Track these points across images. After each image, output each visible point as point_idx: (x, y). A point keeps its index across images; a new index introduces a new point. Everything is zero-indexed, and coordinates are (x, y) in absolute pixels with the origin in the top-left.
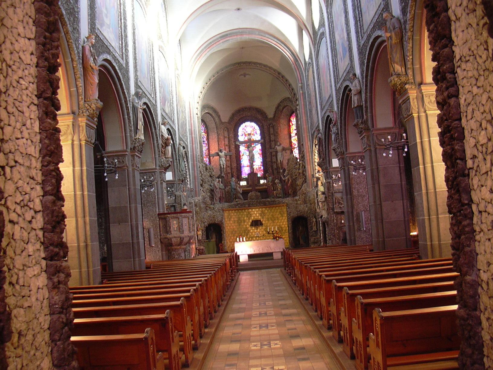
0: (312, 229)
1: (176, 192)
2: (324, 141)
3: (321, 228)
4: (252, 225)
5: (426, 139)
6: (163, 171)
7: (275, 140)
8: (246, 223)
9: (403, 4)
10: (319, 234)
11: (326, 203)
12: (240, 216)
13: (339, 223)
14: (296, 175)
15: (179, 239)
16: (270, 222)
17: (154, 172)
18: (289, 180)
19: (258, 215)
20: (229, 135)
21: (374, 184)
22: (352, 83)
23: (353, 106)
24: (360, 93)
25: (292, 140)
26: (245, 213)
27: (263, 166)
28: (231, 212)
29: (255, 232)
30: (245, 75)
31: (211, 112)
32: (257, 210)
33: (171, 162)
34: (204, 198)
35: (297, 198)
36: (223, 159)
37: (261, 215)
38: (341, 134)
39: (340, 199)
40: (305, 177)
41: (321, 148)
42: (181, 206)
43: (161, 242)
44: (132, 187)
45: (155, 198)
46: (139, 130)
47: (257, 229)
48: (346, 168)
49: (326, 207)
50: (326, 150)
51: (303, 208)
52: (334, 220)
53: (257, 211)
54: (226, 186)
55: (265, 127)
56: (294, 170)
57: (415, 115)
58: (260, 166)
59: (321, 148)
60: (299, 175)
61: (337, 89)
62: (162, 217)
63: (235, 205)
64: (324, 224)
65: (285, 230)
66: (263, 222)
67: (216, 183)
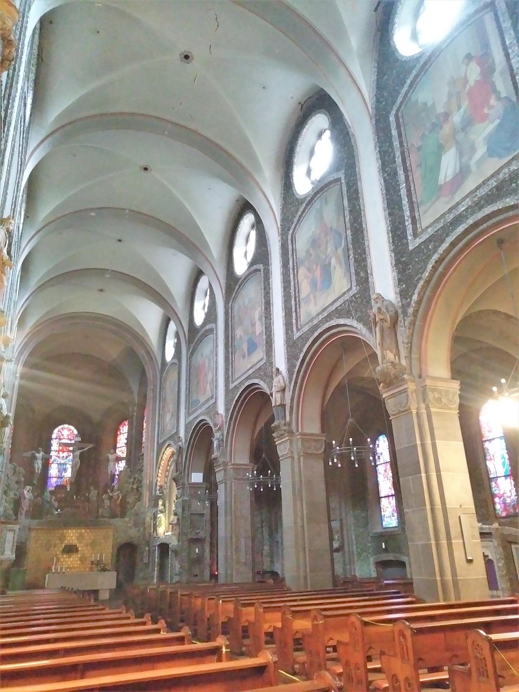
3: (156, 560)
5: (428, 441)
8: (56, 549)
9: (404, 286)
14: (128, 491)
16: (89, 548)
19: (74, 538)
21: (295, 500)
23: (273, 405)
24: (283, 390)
25: (117, 451)
26: (58, 535)
28: (39, 531)
32: (74, 531)
35: (127, 519)
38: (227, 440)
41: (180, 459)
48: (229, 483)
51: (133, 533)
53: (73, 533)
56: (126, 485)
57: (414, 412)
59: (180, 459)
66: (79, 549)
67: (25, 492)
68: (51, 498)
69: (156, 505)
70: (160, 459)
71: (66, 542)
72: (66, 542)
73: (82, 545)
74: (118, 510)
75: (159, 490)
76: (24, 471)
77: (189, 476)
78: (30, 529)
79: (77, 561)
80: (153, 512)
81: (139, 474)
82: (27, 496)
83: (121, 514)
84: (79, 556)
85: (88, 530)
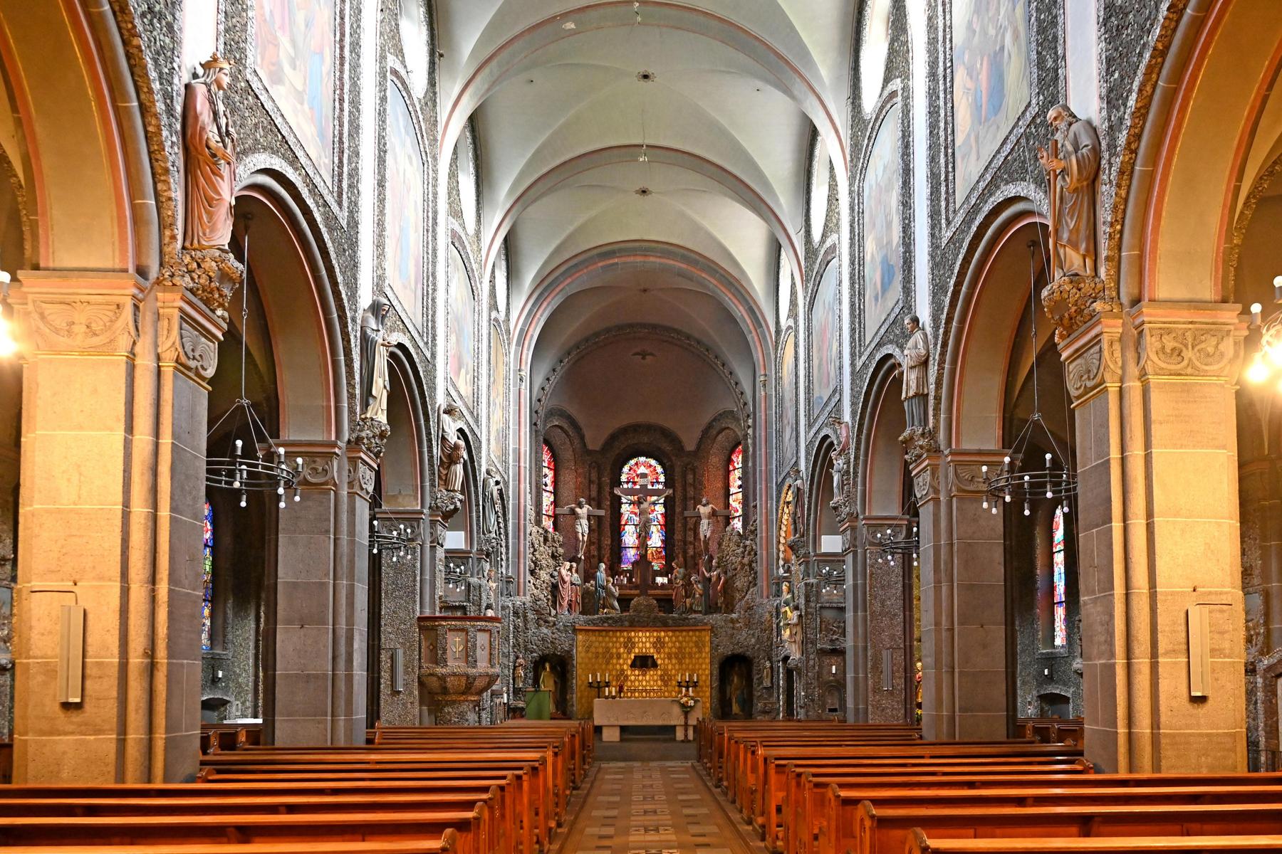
0: (762, 683)
1: (472, 576)
2: (806, 495)
3: (781, 682)
4: (633, 665)
6: (440, 519)
7: (694, 498)
8: (621, 661)
10: (776, 695)
11: (799, 629)
12: (611, 644)
13: (825, 672)
14: (735, 569)
15: (463, 680)
16: (674, 661)
17: (418, 520)
18: (719, 578)
19: (648, 645)
20: (599, 479)
22: (902, 348)
26: (622, 640)
27: (665, 548)
28: (591, 633)
29: (639, 681)
30: (644, 355)
31: (565, 426)
32: (648, 634)
33: (461, 501)
34: (536, 600)
35: (734, 616)
36: (584, 522)
37: (654, 645)
38: (855, 473)
39: (831, 621)
40: (756, 573)
42: (480, 610)
43: (421, 683)
44: (344, 537)
45: (415, 580)
46: (375, 398)
47: (644, 675)
49: (799, 638)
50: (809, 515)
51: (746, 640)
52: (814, 667)
53: (646, 637)
54: (586, 580)
55: (678, 469)
58: (659, 550)
60: (742, 569)
61: (858, 369)
62: (427, 625)
63: (601, 619)
64: (789, 673)
65: (705, 681)
66: (659, 662)
67: (564, 572)
68: (608, 581)
69: (778, 594)
70: (780, 511)
71: (637, 651)
72: (637, 651)
73: (662, 656)
74: (720, 600)
75: (783, 566)
76: (561, 539)
77: (816, 542)
78: (575, 631)
79: (657, 681)
80: (775, 605)
81: (752, 540)
82: (567, 579)
83: (726, 606)
84: (659, 672)
85: (670, 634)
